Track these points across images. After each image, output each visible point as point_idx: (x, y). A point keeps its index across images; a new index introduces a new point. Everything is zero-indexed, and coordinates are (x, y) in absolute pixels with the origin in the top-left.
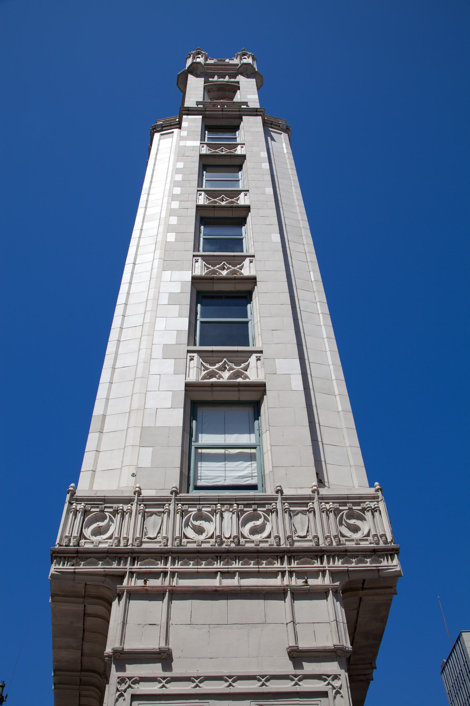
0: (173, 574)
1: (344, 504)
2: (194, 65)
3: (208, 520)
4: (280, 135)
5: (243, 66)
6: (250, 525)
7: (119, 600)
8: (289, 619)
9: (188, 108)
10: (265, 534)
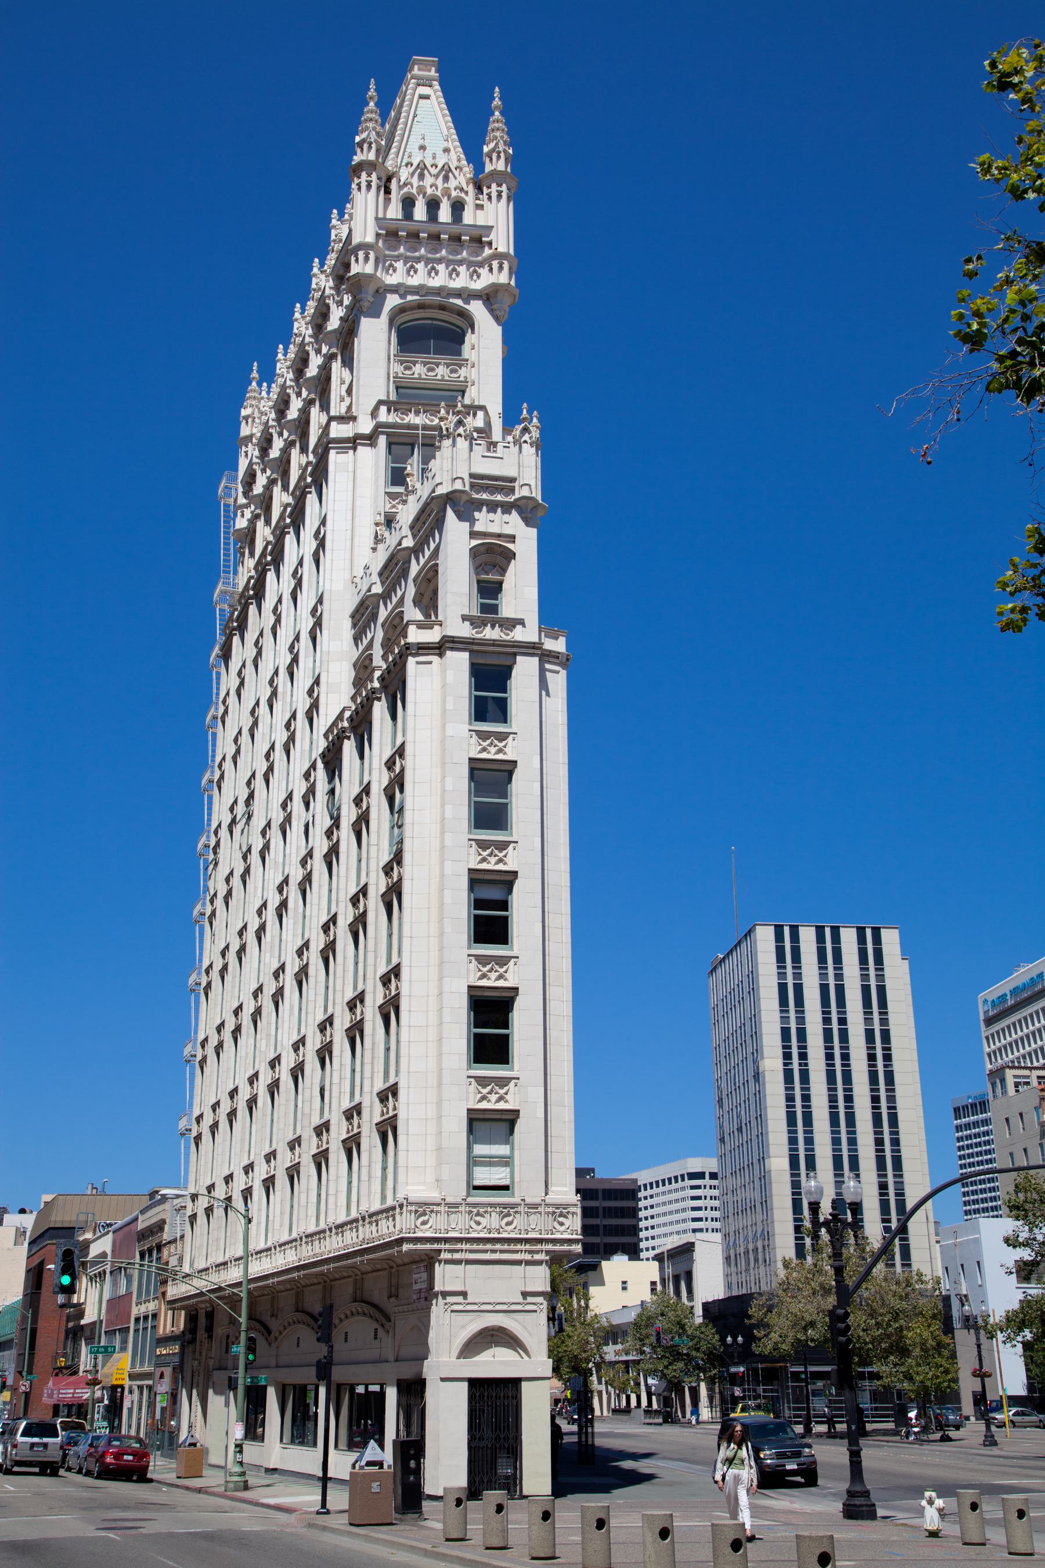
0: (466, 1251)
1: (558, 1208)
2: (457, 494)
3: (483, 1216)
5: (525, 501)
6: (506, 1220)
8: (523, 1276)
9: (453, 637)
10: (513, 1226)
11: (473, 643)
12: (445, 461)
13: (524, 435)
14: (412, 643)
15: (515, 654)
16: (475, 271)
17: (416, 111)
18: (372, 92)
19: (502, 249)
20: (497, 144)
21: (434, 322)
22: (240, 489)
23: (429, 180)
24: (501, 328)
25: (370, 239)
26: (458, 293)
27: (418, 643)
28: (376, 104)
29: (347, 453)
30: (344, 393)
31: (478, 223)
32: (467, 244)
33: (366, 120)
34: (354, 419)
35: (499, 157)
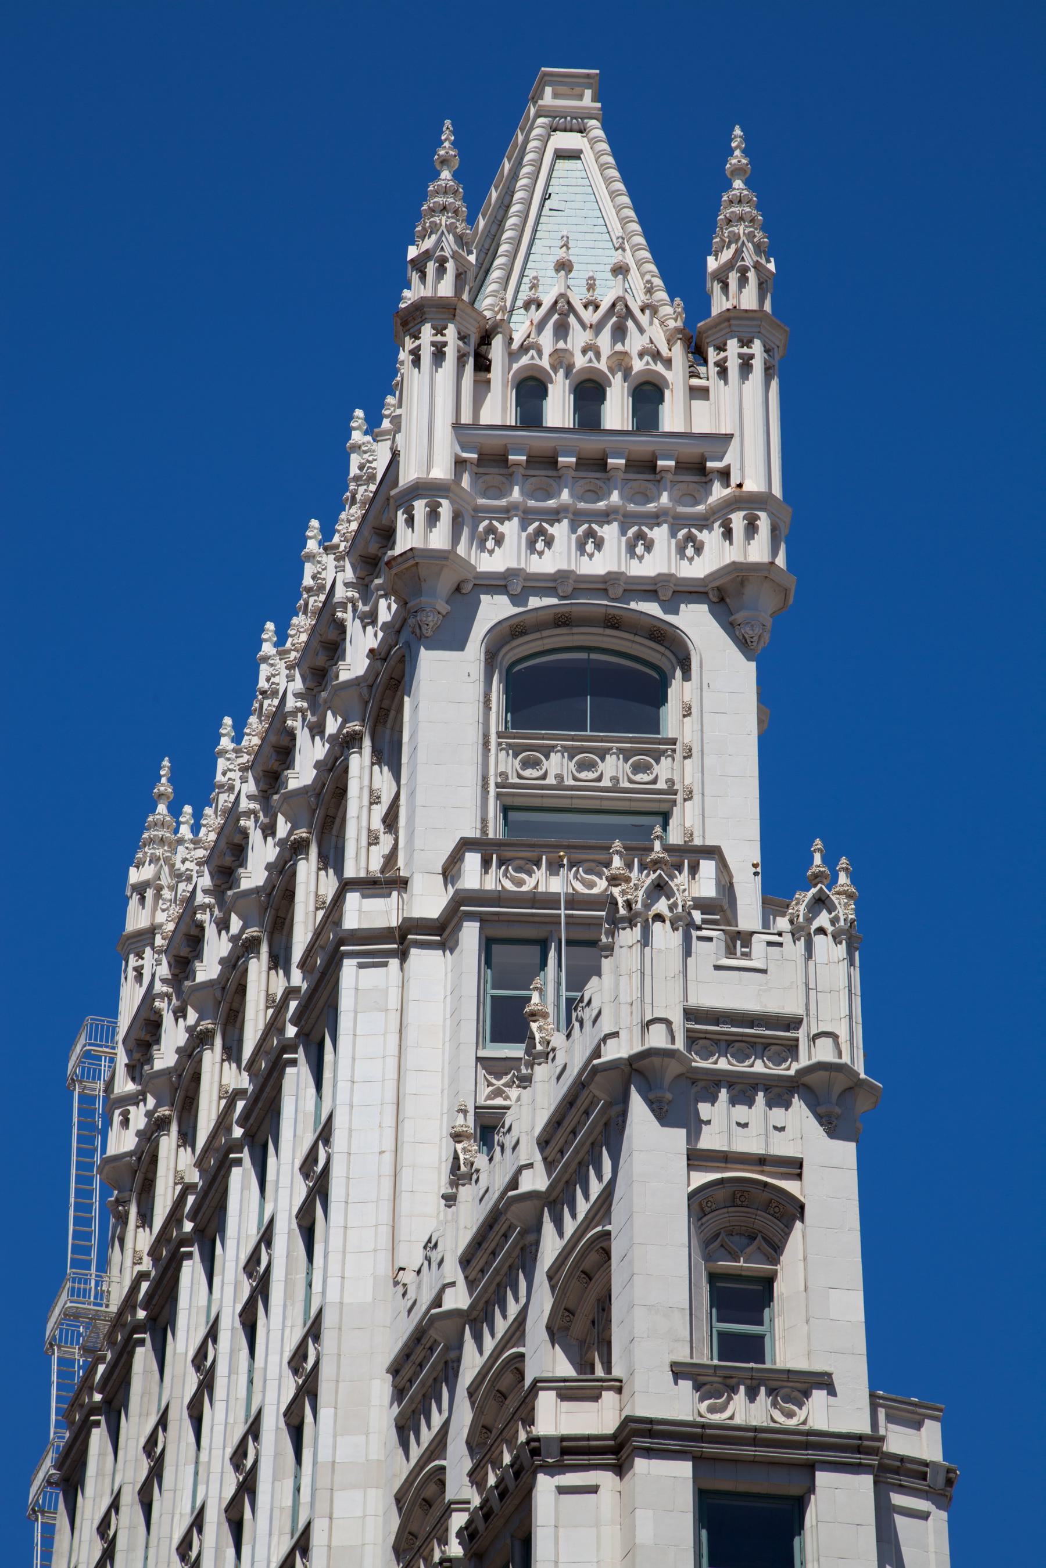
2: (656, 1060)
4: (923, 1522)
5: (823, 1074)
9: (651, 1421)
11: (701, 1438)
12: (624, 980)
13: (816, 915)
14: (549, 1439)
15: (811, 1467)
16: (690, 538)
17: (547, 185)
18: (446, 149)
19: (752, 485)
20: (738, 253)
21: (594, 656)
22: (122, 1058)
23: (578, 338)
24: (753, 665)
25: (441, 471)
26: (650, 589)
27: (563, 1439)
28: (456, 176)
29: (385, 965)
30: (377, 824)
31: (696, 430)
32: (669, 476)
33: (432, 210)
34: (402, 884)
35: (743, 281)
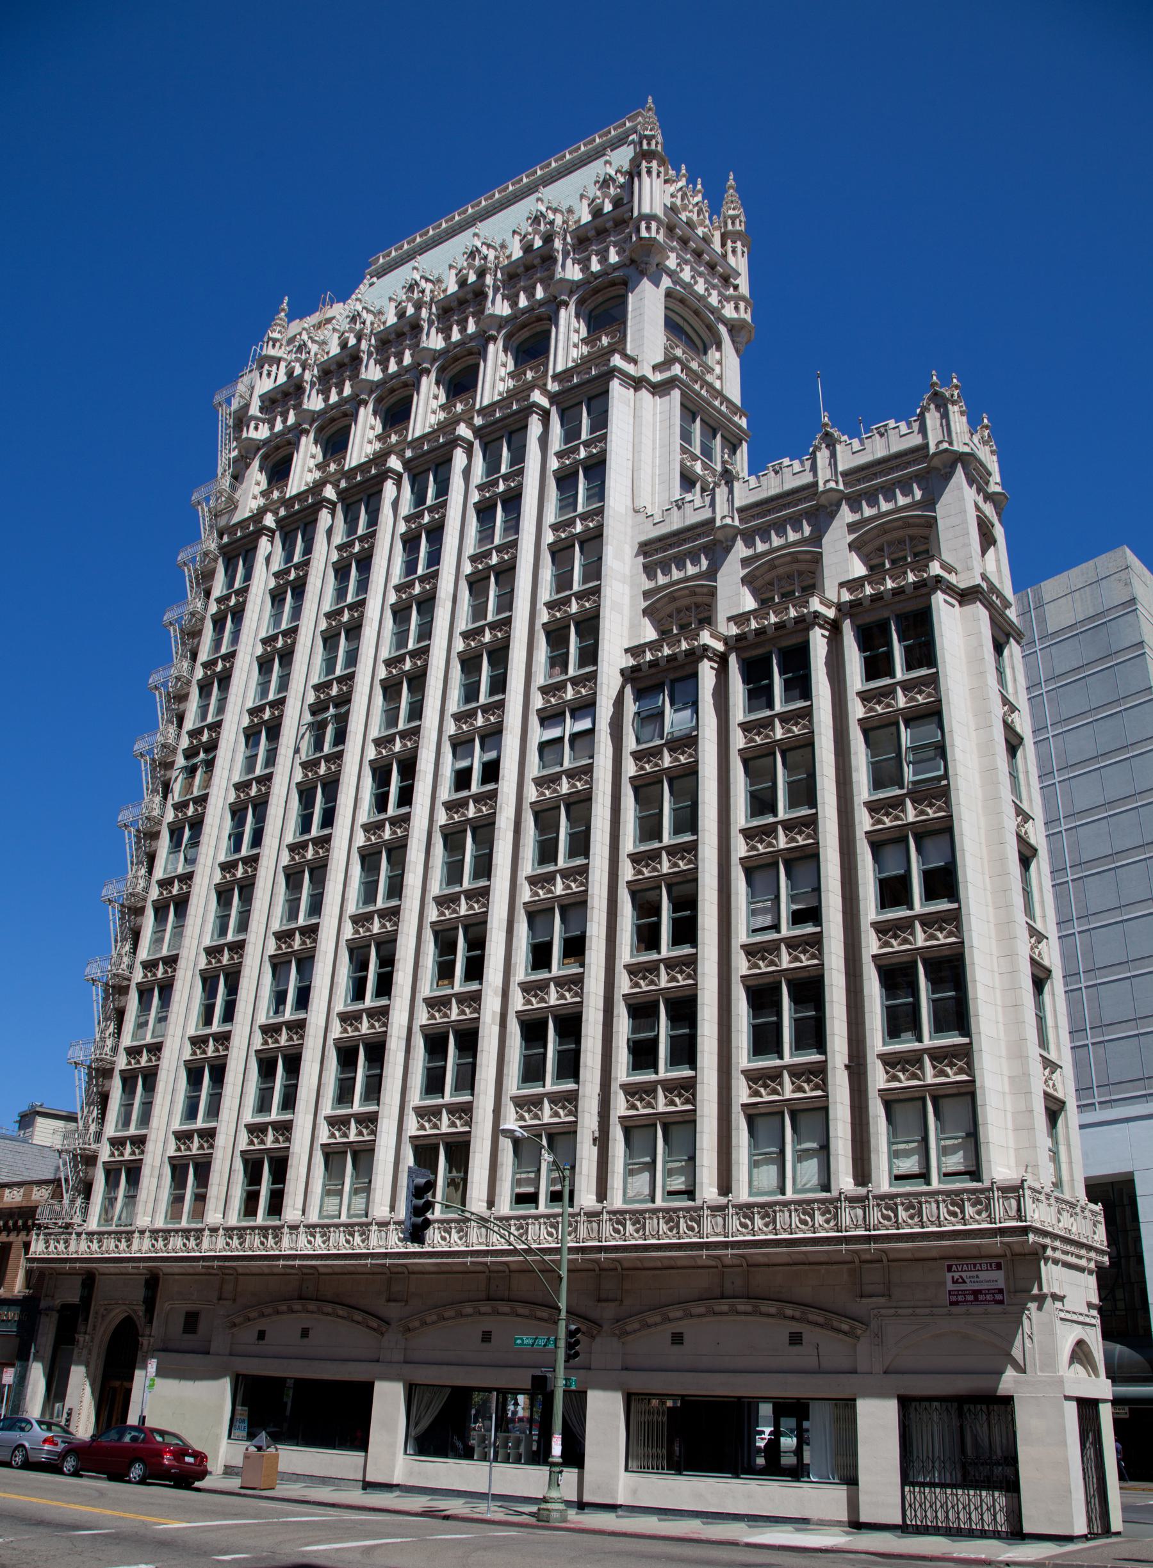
7: (1046, 1264)
